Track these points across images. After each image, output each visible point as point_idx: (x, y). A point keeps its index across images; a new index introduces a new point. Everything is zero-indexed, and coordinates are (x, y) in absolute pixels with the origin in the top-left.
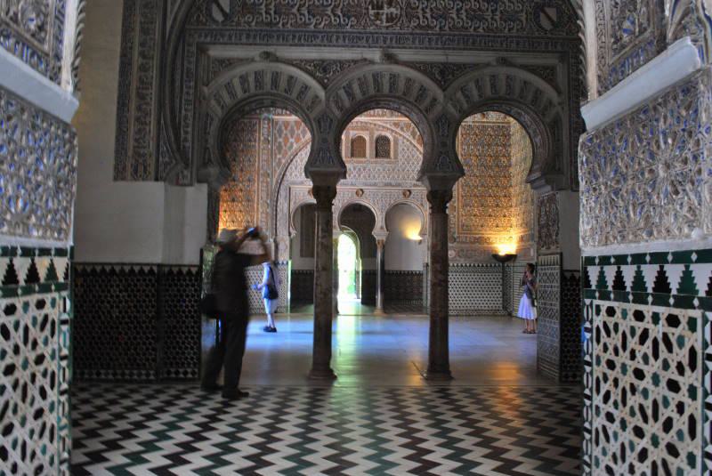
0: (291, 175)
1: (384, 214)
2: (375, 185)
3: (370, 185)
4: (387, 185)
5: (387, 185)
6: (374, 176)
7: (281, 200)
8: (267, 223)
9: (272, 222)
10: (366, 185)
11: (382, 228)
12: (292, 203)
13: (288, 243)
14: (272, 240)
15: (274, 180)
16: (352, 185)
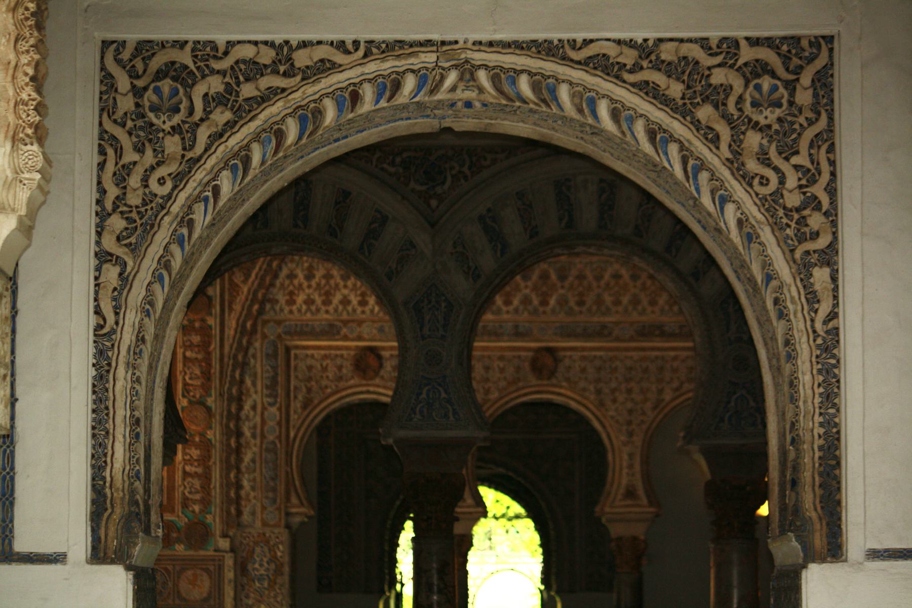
0: (291, 302)
1: (638, 440)
2: (602, 332)
3: (587, 334)
4: (645, 332)
5: (645, 332)
6: (599, 301)
7: (256, 396)
8: (206, 477)
9: (225, 475)
10: (568, 332)
11: (630, 493)
12: (296, 405)
13: (282, 552)
14: (224, 544)
15: (232, 323)
16: (518, 334)
